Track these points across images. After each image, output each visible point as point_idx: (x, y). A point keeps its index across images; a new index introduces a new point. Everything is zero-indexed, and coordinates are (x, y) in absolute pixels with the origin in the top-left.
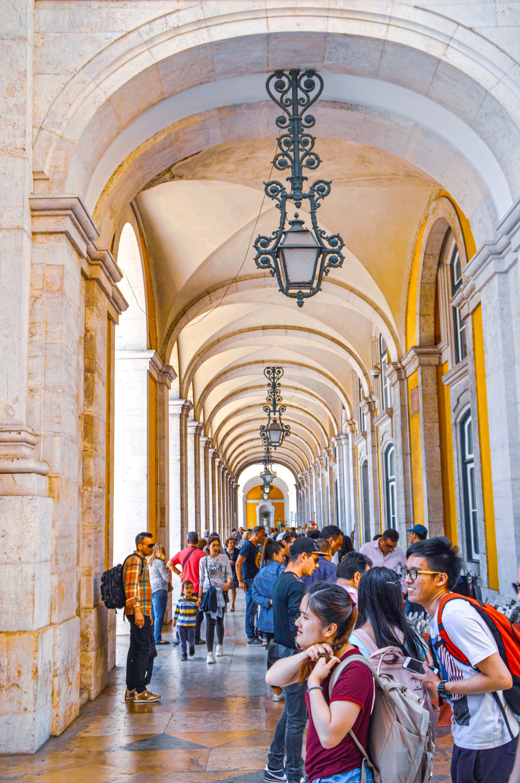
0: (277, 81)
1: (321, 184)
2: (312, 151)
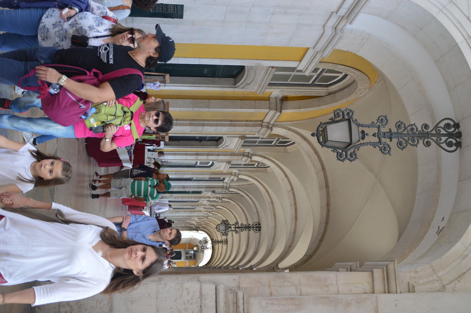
0: (450, 125)
1: (388, 149)
2: (408, 145)
